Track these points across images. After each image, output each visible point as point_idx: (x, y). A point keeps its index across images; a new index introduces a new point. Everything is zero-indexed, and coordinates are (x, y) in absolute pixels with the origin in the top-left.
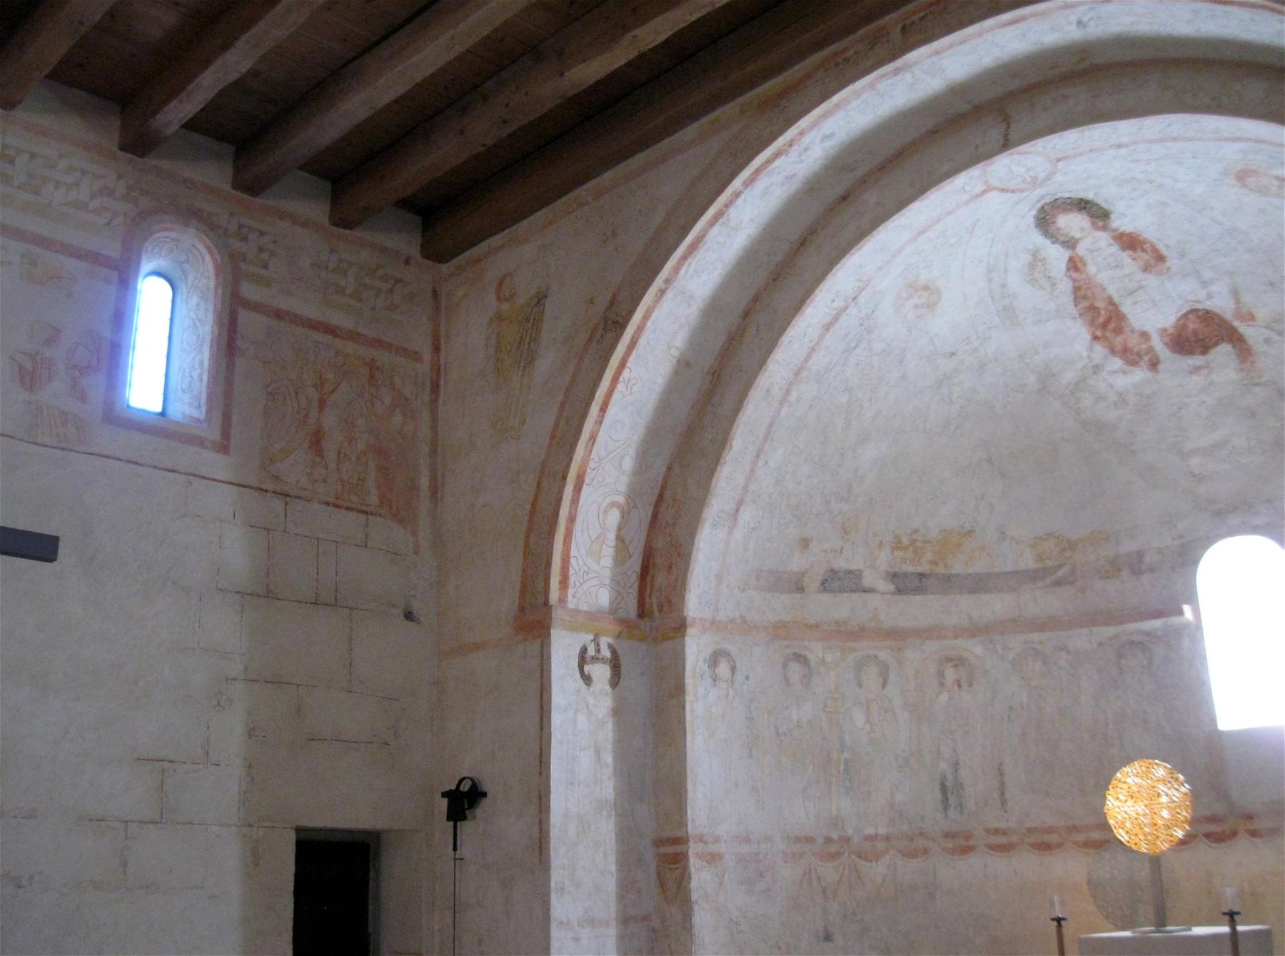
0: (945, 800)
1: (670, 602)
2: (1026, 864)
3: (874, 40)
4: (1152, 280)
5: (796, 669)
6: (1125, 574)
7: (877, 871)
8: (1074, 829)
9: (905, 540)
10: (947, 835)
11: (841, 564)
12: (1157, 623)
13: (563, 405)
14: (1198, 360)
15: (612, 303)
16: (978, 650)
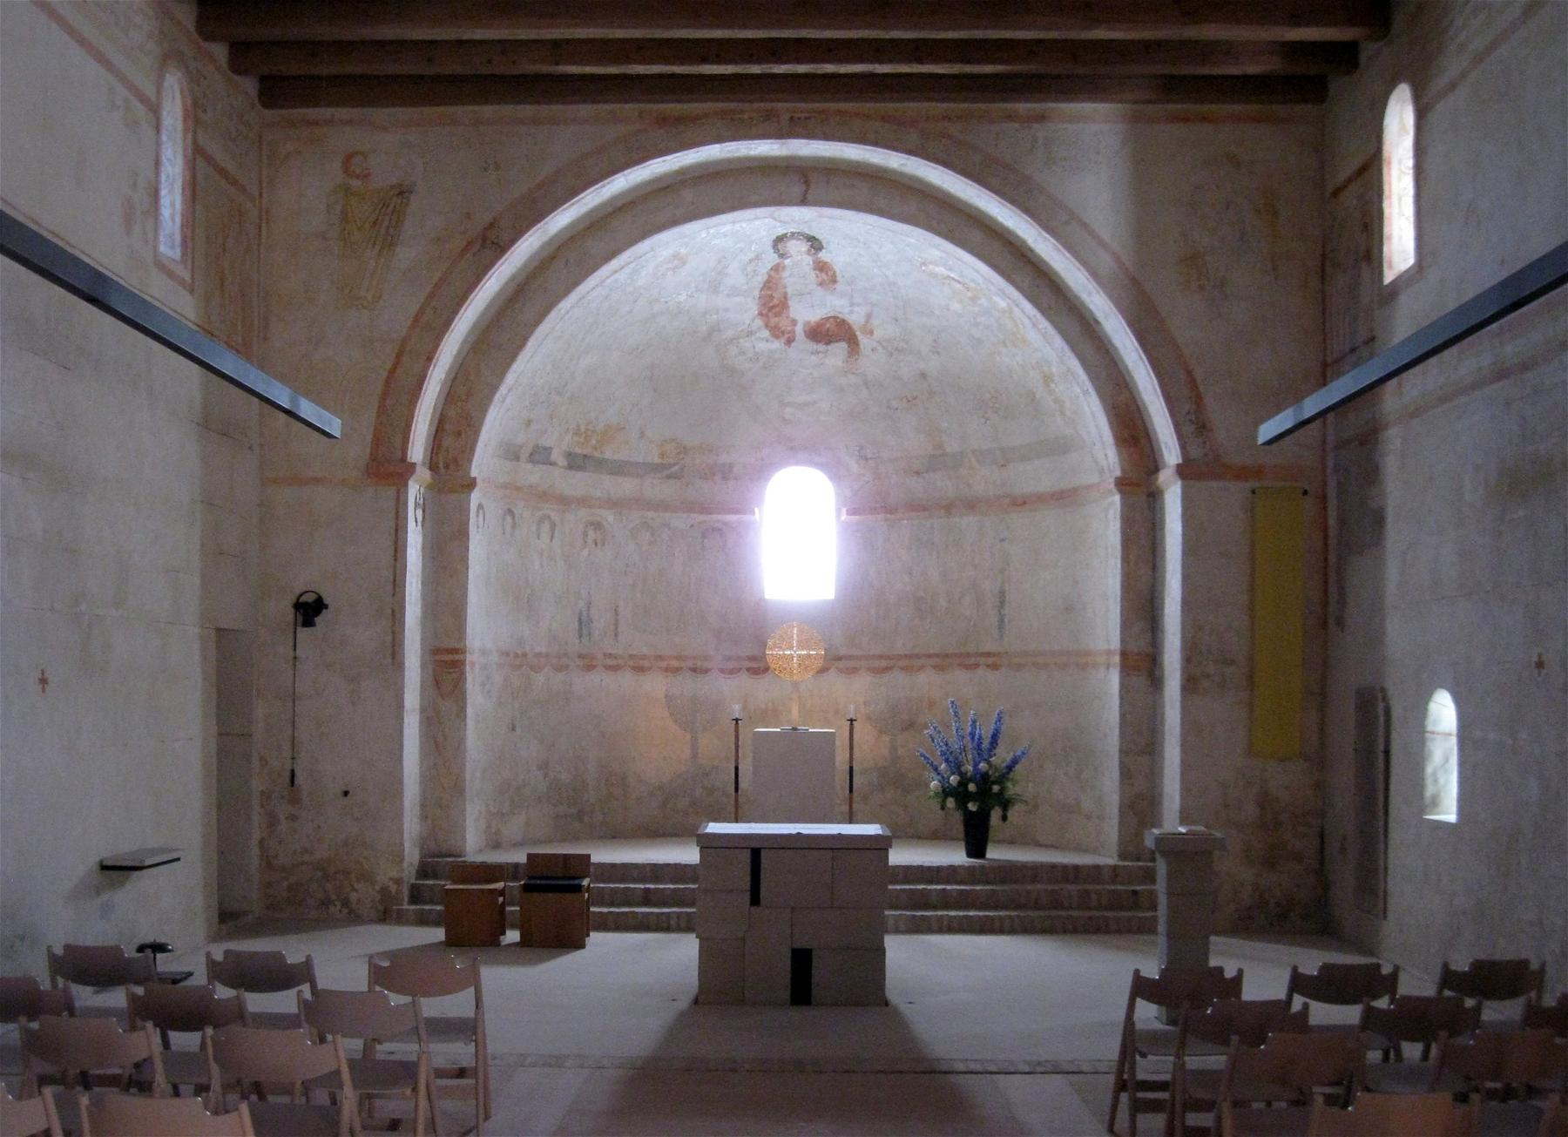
0: (580, 629)
1: (455, 461)
2: (627, 679)
3: (769, 116)
4: (820, 292)
5: (509, 518)
6: (718, 477)
7: (540, 679)
8: (660, 658)
9: (583, 428)
10: (580, 656)
11: (545, 442)
12: (732, 518)
13: (431, 296)
14: (821, 347)
15: (491, 225)
16: (611, 518)
